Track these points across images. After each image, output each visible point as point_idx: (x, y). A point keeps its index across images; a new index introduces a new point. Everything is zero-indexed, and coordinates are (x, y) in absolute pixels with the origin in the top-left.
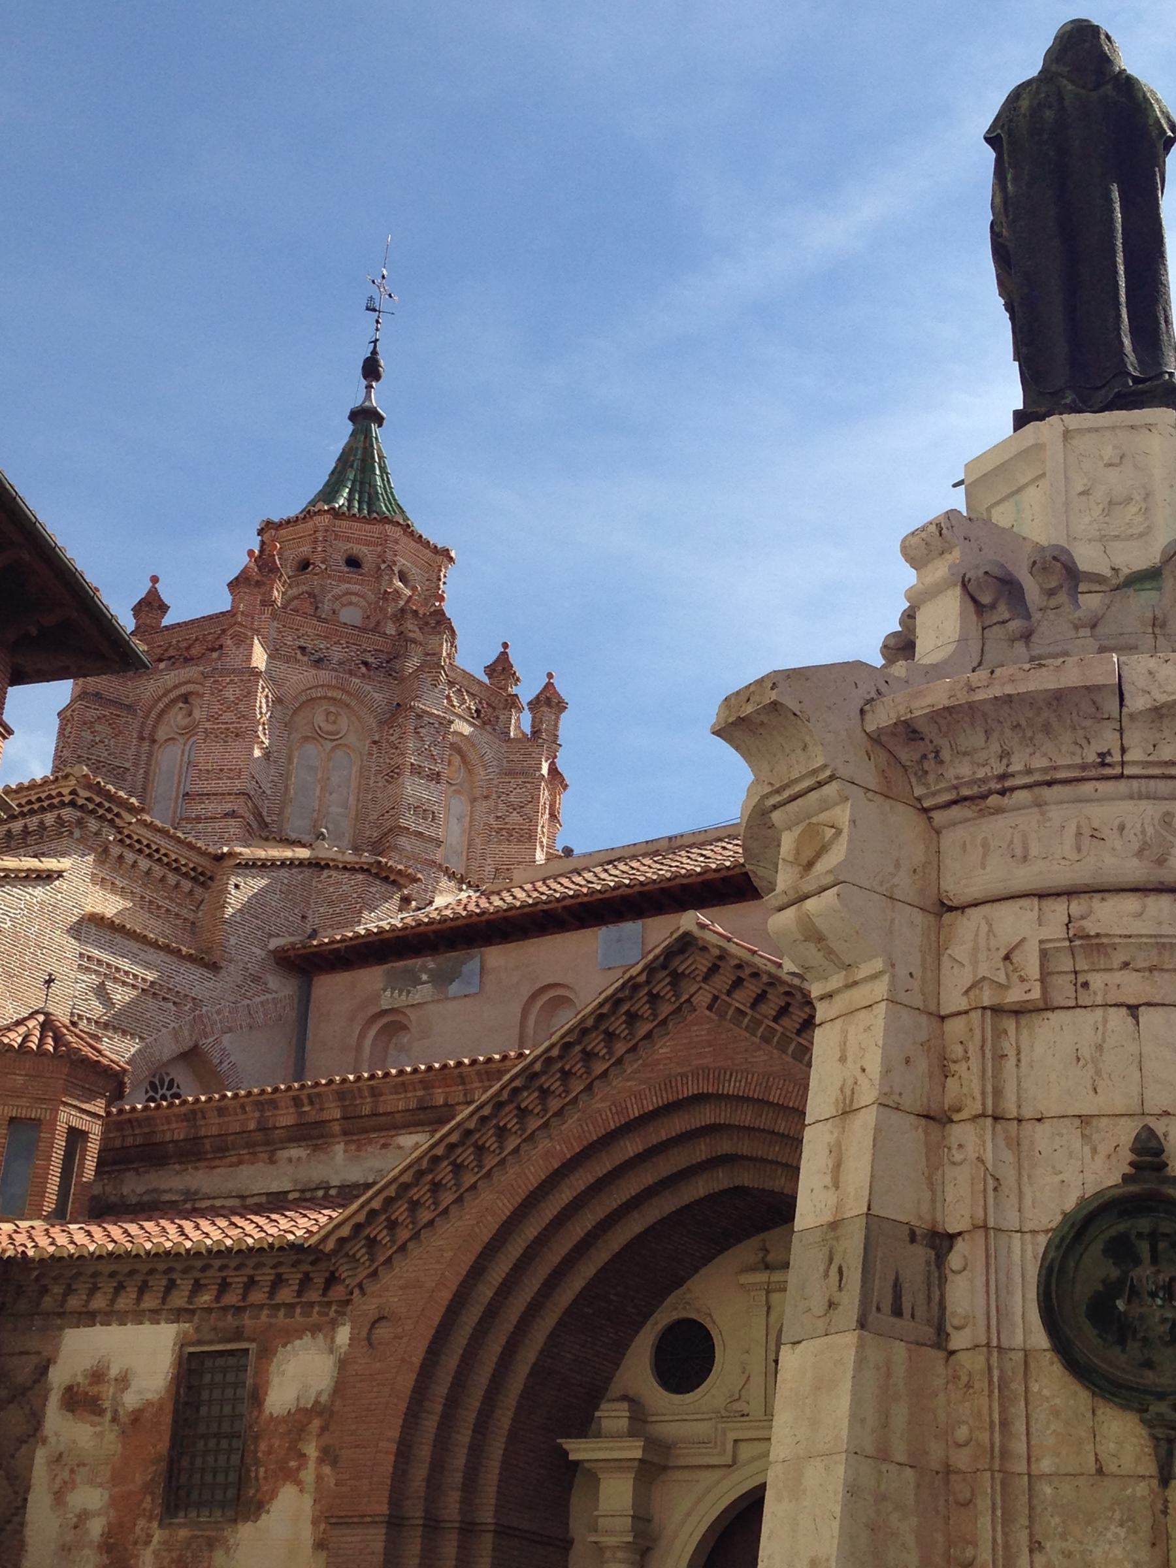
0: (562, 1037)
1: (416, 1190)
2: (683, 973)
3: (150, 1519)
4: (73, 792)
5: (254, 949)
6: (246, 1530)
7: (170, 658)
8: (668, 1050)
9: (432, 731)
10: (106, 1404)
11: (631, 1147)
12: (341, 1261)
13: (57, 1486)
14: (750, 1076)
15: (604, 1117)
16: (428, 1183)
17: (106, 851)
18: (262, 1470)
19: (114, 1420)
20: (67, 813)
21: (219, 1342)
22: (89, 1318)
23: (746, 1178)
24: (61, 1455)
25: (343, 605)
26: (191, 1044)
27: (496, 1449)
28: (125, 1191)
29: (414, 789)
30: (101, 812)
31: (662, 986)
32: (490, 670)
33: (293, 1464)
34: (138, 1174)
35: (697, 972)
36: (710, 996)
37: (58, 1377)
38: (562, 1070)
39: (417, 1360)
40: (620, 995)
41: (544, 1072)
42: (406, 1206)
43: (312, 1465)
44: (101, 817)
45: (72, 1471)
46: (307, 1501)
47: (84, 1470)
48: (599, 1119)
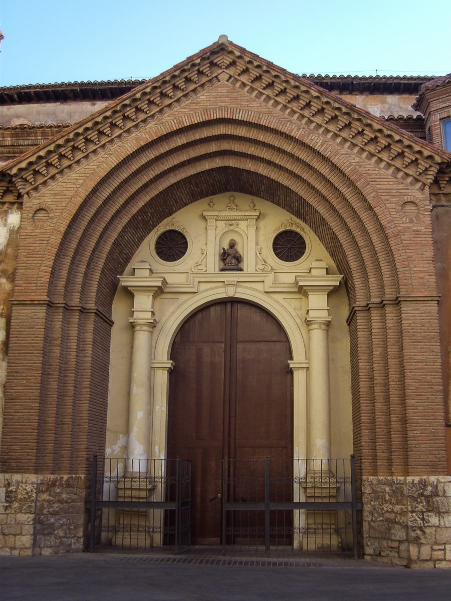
1: (64, 149)
2: (216, 63)
8: (205, 97)
11: (180, 141)
12: (19, 180)
14: (250, 112)
15: (170, 124)
16: (71, 146)
23: (232, 162)
27: (97, 276)
35: (223, 64)
36: (228, 76)
39: (63, 229)
42: (57, 156)
48: (167, 125)
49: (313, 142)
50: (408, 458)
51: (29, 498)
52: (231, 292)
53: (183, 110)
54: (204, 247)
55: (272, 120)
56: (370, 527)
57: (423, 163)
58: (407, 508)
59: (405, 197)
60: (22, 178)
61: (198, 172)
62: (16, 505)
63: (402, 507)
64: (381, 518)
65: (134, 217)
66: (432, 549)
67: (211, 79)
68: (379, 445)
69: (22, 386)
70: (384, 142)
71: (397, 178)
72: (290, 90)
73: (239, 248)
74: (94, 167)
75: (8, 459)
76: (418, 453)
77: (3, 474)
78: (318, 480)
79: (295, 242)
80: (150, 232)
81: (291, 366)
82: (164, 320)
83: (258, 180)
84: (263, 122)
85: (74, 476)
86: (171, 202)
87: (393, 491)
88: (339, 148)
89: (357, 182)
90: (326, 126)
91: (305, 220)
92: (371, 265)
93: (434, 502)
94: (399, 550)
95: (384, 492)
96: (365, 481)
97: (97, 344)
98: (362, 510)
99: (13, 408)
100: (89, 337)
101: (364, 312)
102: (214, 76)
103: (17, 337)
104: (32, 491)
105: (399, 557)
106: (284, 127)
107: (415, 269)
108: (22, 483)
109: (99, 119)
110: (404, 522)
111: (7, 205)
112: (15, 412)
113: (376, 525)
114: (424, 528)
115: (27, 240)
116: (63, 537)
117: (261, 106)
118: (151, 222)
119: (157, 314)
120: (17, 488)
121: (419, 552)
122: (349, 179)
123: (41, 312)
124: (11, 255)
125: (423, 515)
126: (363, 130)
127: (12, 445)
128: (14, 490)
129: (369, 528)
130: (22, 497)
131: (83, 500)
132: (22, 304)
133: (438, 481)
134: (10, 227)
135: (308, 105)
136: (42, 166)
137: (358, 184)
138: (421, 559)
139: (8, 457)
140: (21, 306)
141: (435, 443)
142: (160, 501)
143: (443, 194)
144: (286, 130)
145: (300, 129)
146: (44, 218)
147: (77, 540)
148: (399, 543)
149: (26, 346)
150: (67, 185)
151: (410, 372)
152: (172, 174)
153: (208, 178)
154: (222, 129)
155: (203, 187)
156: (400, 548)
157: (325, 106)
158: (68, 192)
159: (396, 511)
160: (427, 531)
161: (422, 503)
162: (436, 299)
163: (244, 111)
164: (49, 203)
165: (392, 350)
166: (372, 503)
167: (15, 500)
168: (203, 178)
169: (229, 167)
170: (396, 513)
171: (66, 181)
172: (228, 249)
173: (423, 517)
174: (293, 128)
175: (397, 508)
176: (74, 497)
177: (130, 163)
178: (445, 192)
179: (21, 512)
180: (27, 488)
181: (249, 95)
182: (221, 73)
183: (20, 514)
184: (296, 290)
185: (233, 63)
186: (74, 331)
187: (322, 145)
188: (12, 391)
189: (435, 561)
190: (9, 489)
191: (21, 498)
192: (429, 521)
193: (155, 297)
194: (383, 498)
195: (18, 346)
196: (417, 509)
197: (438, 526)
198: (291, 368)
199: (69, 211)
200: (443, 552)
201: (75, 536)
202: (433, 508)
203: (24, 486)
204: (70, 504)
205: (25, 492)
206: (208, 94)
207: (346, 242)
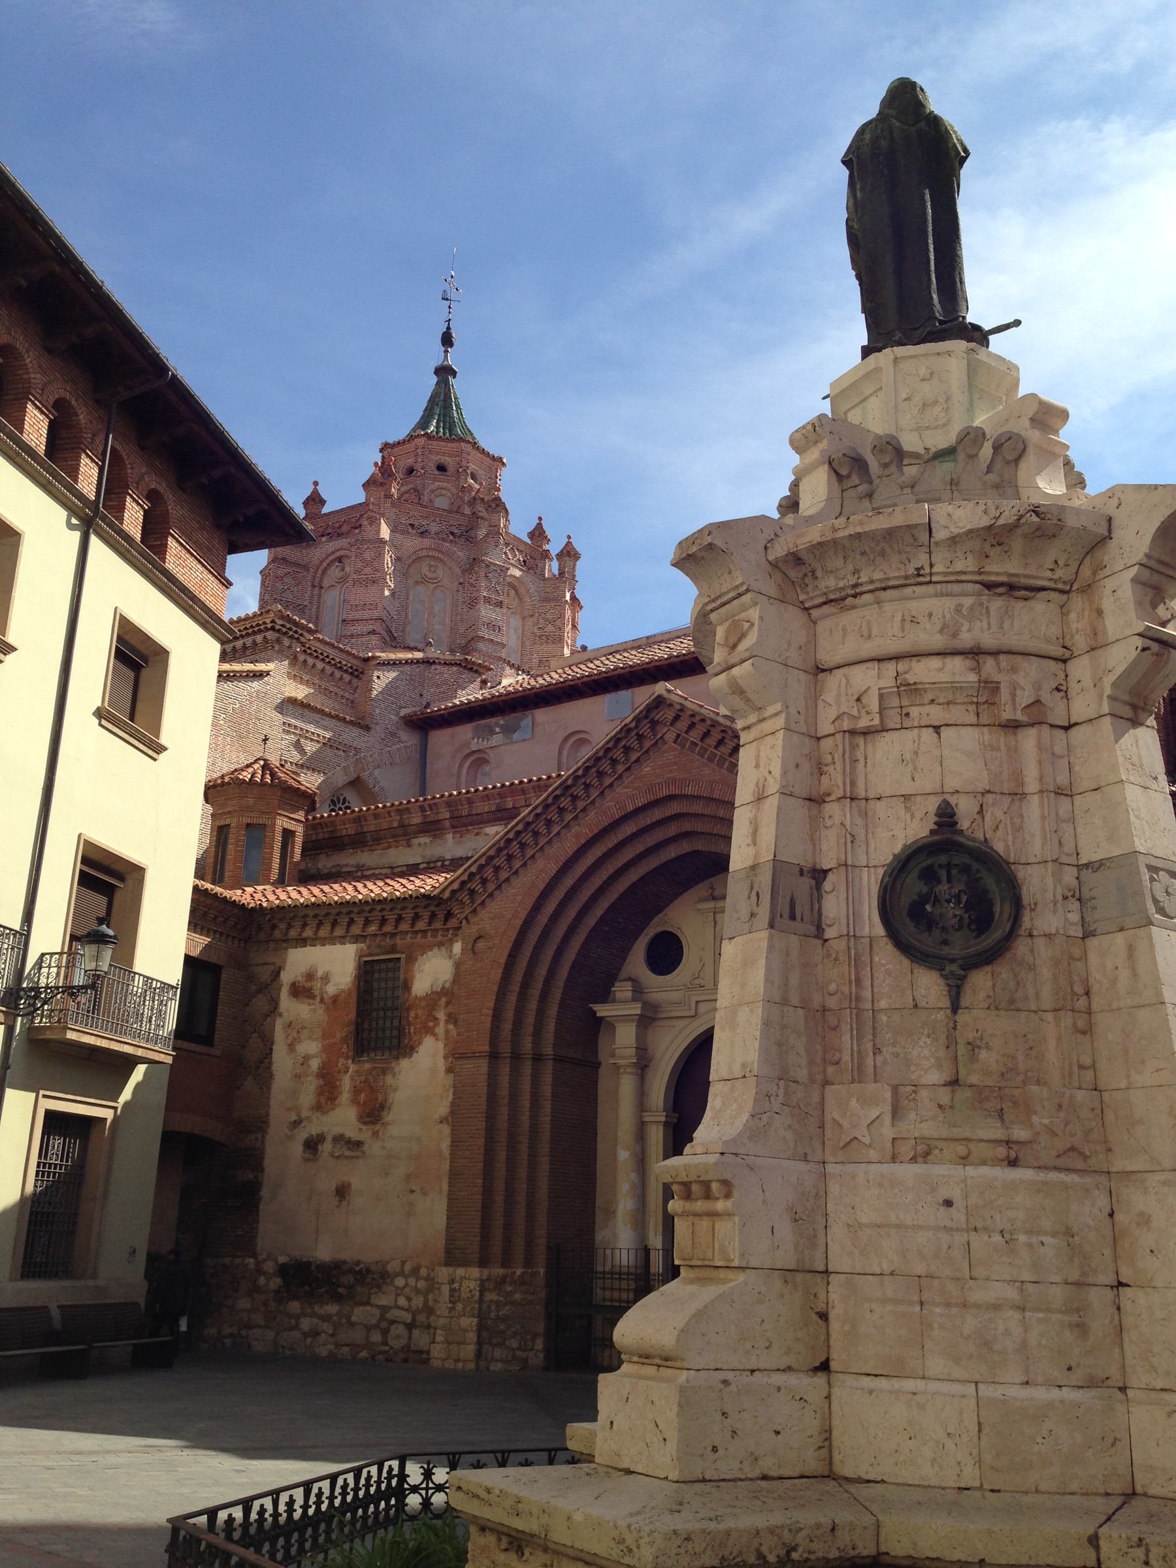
3: (347, 1058)
4: (273, 621)
5: (391, 716)
6: (404, 1063)
7: (328, 534)
8: (649, 769)
9: (497, 575)
10: (317, 993)
11: (629, 829)
13: (289, 1042)
17: (295, 658)
18: (412, 1028)
19: (322, 1001)
20: (270, 635)
21: (383, 954)
22: (303, 942)
23: (700, 845)
24: (291, 1023)
25: (437, 496)
26: (356, 776)
27: (553, 1011)
28: (320, 866)
29: (486, 612)
30: (291, 633)
31: (645, 729)
32: (531, 535)
33: (431, 1024)
34: (327, 856)
37: (286, 977)
39: (503, 961)
40: (619, 736)
41: (573, 785)
43: (442, 1024)
44: (291, 637)
45: (298, 1032)
46: (441, 1045)
47: (305, 1031)
62: (459, 1306)
116: (517, 1349)
120: (461, 1285)
176: (530, 1297)
179: (464, 1315)
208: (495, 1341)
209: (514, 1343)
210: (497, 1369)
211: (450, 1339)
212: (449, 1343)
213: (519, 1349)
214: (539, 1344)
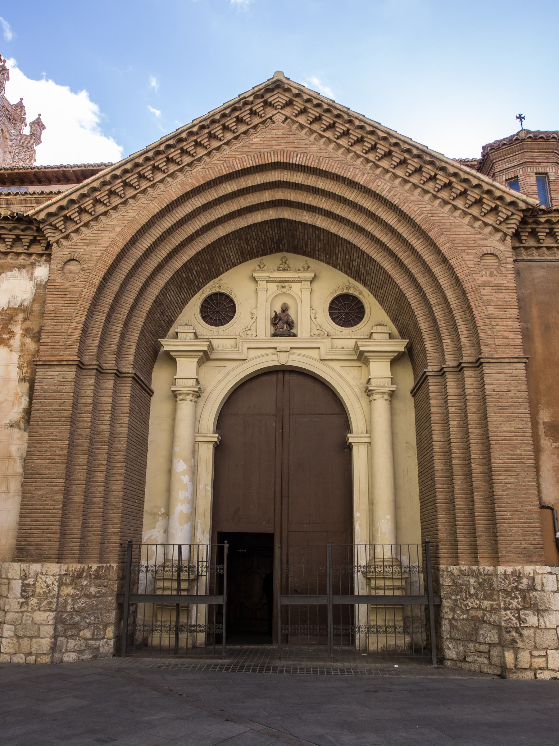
0: (200, 122)
1: (99, 193)
2: (270, 102)
8: (259, 140)
12: (47, 227)
14: (308, 156)
15: (219, 168)
23: (287, 214)
27: (134, 336)
33: (5, 336)
35: (278, 103)
36: (284, 117)
38: (196, 141)
39: (97, 281)
41: (186, 140)
42: (91, 201)
46: (15, 357)
48: (216, 169)
49: (379, 189)
50: (497, 544)
51: (49, 593)
52: (283, 360)
53: (234, 153)
54: (254, 311)
55: (333, 164)
56: (452, 627)
57: (504, 211)
58: (499, 605)
59: (484, 249)
60: (51, 225)
61: (249, 224)
62: (33, 601)
63: (492, 602)
64: (465, 616)
65: (177, 273)
66: (531, 655)
67: (265, 121)
68: (460, 528)
69: (45, 459)
70: (459, 188)
71: (474, 228)
72: (353, 130)
73: (291, 313)
74: (133, 214)
75: (25, 545)
76: (509, 538)
77: (19, 564)
78: (388, 570)
79: (353, 307)
80: (195, 295)
81: (351, 440)
82: (209, 389)
83: (314, 235)
84: (323, 167)
85: (105, 565)
86: (219, 261)
87: (480, 584)
88: (409, 195)
89: (429, 232)
90: (394, 171)
91: (364, 283)
92: (444, 325)
93: (530, 598)
94: (489, 655)
95: (468, 584)
96: (443, 571)
97: (135, 413)
98: (440, 605)
99: (34, 484)
100: (125, 404)
101: (437, 377)
102: (268, 116)
103: (40, 402)
104: (53, 584)
105: (490, 663)
106: (347, 171)
107: (497, 327)
108: (42, 573)
109: (140, 160)
110: (495, 621)
111: (34, 257)
112: (35, 489)
113: (459, 624)
114: (520, 629)
115: (55, 293)
116: (90, 639)
117: (321, 149)
118: (196, 282)
119: (201, 382)
121: (516, 659)
122: (420, 228)
123: (70, 374)
124: (38, 311)
125: (519, 613)
126: (436, 175)
127: (31, 529)
128: (32, 583)
129: (451, 628)
130: (41, 592)
131: (115, 593)
132: (49, 364)
133: (535, 571)
134: (37, 281)
135: (374, 148)
136: (74, 211)
137: (431, 234)
138: (519, 666)
139: (26, 543)
140: (47, 367)
141: (529, 527)
142: (204, 594)
143: (524, 247)
144: (349, 175)
145: (364, 174)
146: (75, 270)
147: (107, 642)
148: (490, 647)
149: (51, 413)
150: (102, 233)
151: (496, 443)
152: (220, 227)
153: (259, 233)
154: (276, 176)
155: (254, 244)
156: (491, 653)
157: (392, 149)
158: (103, 241)
159: (484, 607)
160: (525, 632)
161: (517, 598)
162: (524, 360)
163: (302, 155)
164: (82, 253)
165: (473, 419)
166: (453, 598)
167: (32, 596)
168: (254, 233)
169: (284, 219)
170: (483, 610)
171: (102, 229)
172: (280, 314)
173: (519, 615)
174: (357, 173)
175: (486, 604)
176: (104, 590)
177: (174, 211)
178: (526, 245)
179: (39, 609)
180: (47, 580)
181: (307, 137)
182: (275, 114)
183: (38, 612)
184: (355, 357)
185: (290, 103)
186: (107, 398)
187: (389, 192)
188: (33, 465)
189: (535, 670)
190: (25, 582)
191: (39, 593)
192: (526, 620)
193: (200, 363)
194: (467, 591)
195: (42, 413)
196: (511, 606)
197: (537, 627)
198: (350, 443)
199: (105, 261)
200: (545, 659)
201: (104, 638)
202: (531, 605)
203: (43, 577)
204: (99, 599)
205: (45, 585)
206: (261, 137)
207: (415, 301)
208: (69, 633)
209: (87, 633)
210: (71, 660)
211: (21, 633)
212: (18, 637)
213: (93, 639)
214: (110, 632)
